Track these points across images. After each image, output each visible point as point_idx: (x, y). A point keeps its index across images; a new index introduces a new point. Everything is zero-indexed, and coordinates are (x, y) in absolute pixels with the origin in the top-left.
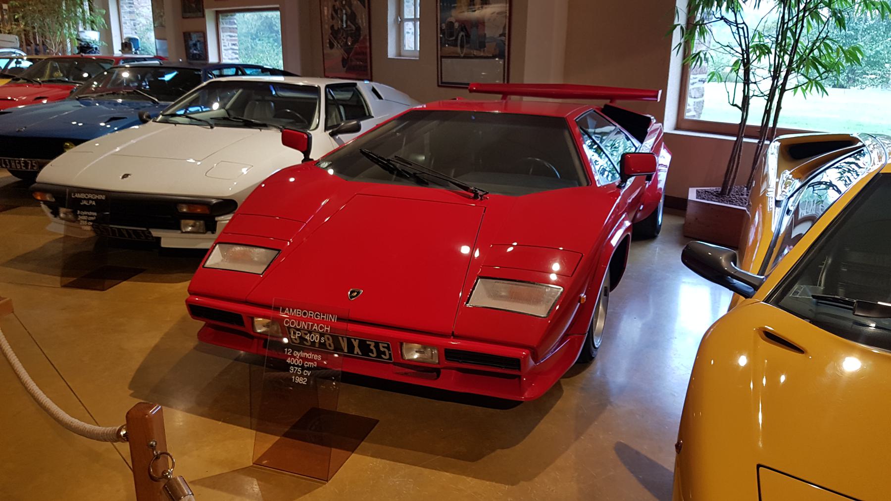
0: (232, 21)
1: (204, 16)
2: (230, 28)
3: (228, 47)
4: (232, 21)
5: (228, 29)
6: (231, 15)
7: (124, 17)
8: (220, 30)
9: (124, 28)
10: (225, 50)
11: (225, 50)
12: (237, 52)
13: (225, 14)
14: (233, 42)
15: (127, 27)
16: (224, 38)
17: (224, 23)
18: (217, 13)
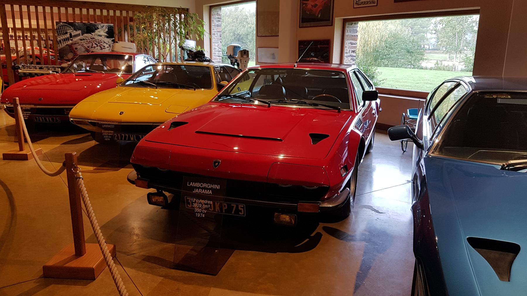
0: (355, 29)
1: (332, 24)
2: (352, 35)
3: (349, 54)
4: (355, 29)
5: (351, 36)
6: (355, 24)
7: (214, 30)
8: (345, 37)
9: (213, 38)
10: (346, 57)
11: (346, 57)
12: (355, 58)
13: (351, 23)
14: (353, 50)
15: (215, 38)
16: (347, 45)
17: (349, 31)
18: (345, 21)
